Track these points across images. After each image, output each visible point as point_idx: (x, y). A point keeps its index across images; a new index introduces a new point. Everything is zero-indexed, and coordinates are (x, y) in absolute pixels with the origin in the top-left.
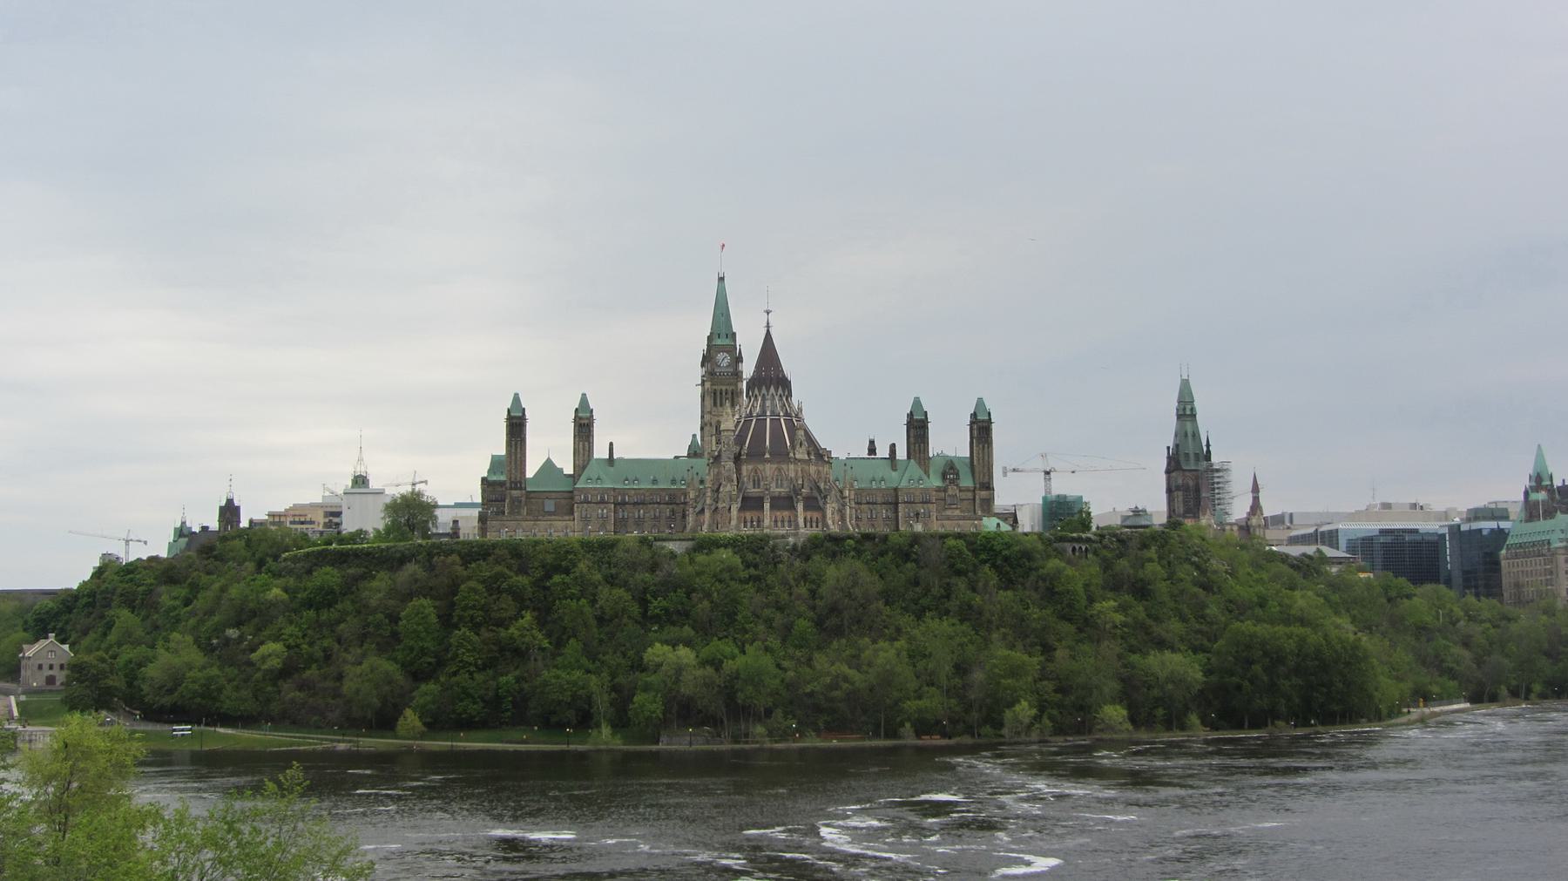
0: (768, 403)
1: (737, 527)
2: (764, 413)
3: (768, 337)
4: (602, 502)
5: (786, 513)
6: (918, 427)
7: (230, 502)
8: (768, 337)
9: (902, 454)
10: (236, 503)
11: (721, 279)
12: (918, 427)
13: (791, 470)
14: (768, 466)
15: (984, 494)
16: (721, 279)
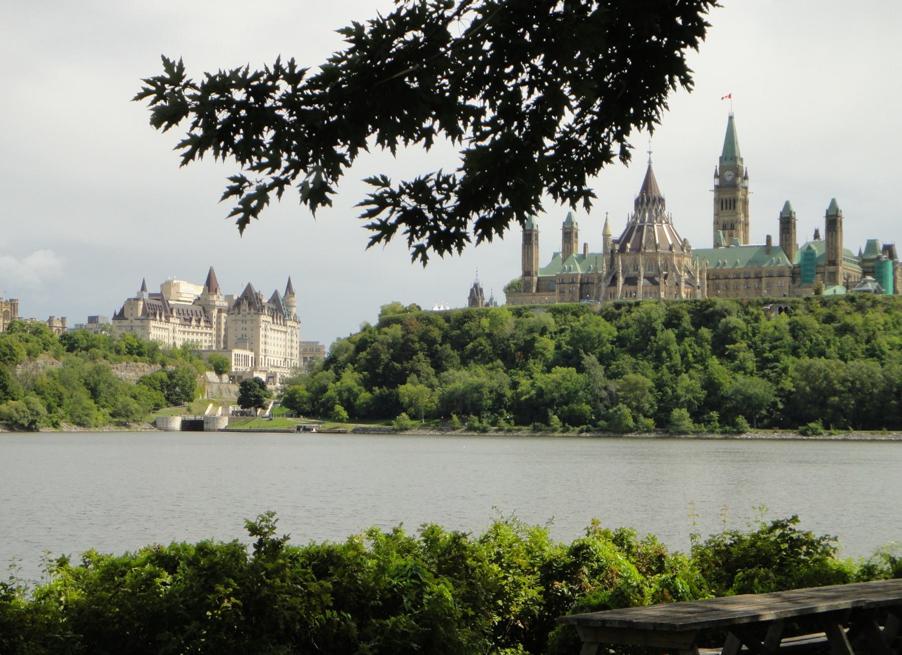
0: (647, 215)
1: (621, 297)
2: (643, 221)
3: (649, 170)
4: (573, 282)
5: (632, 288)
6: (787, 222)
7: (476, 286)
8: (649, 170)
9: (776, 242)
10: (481, 286)
11: (731, 118)
12: (787, 222)
13: (641, 259)
14: (627, 257)
15: (831, 268)
16: (731, 118)
